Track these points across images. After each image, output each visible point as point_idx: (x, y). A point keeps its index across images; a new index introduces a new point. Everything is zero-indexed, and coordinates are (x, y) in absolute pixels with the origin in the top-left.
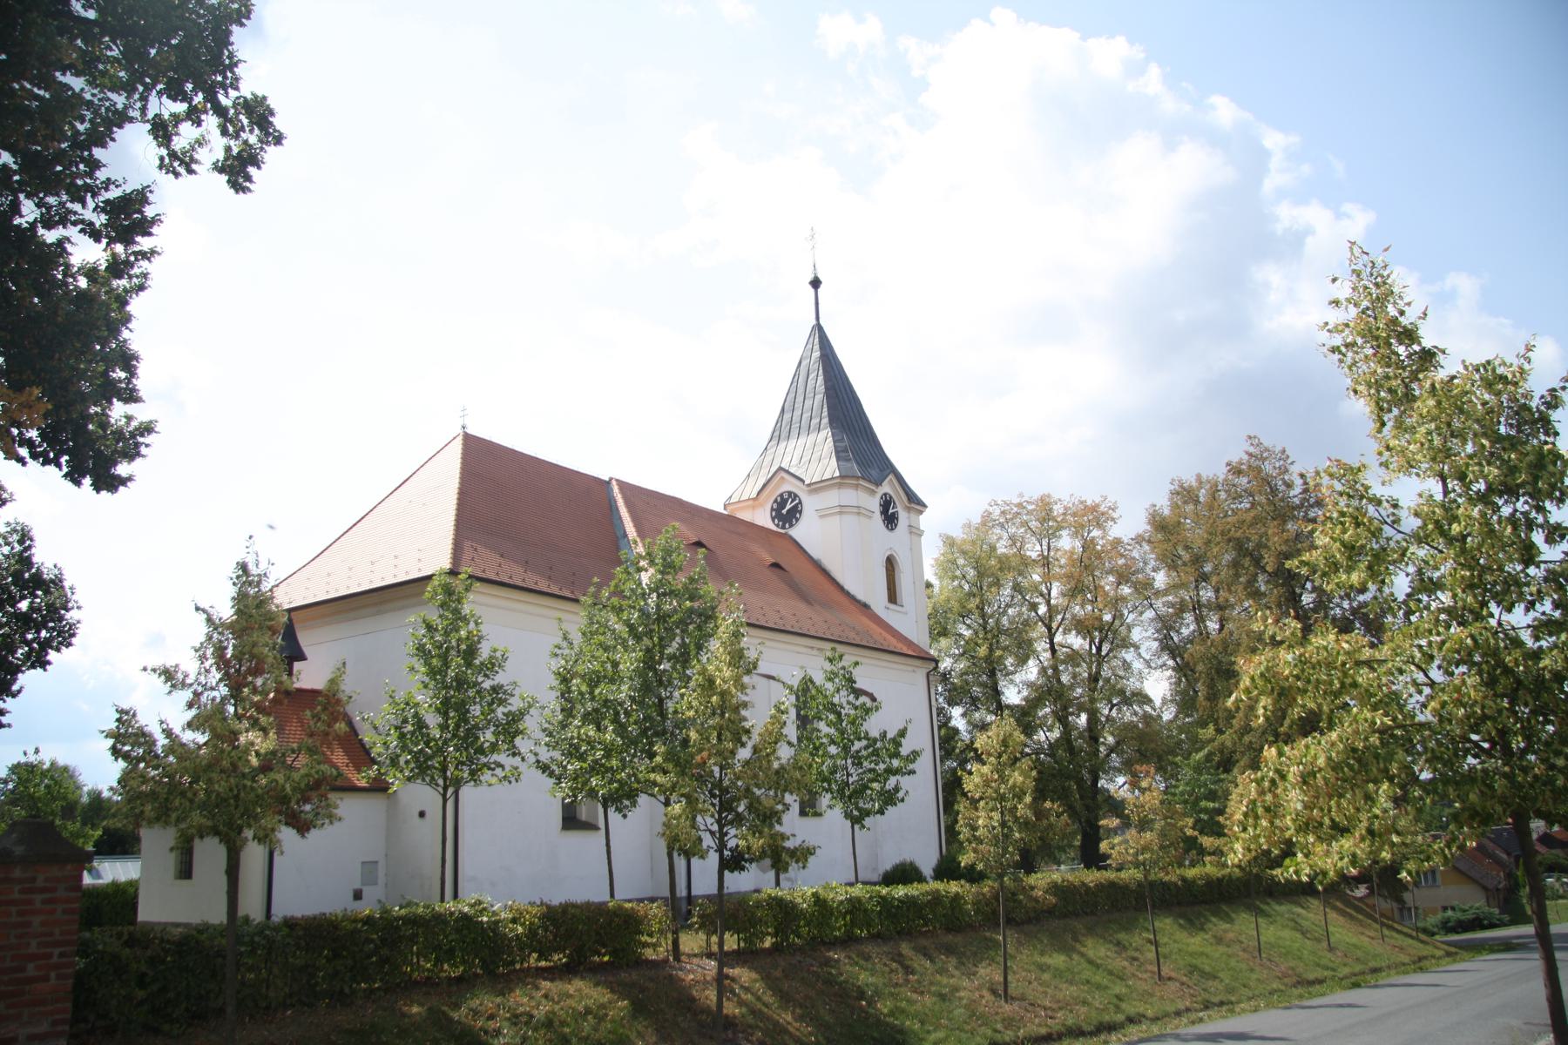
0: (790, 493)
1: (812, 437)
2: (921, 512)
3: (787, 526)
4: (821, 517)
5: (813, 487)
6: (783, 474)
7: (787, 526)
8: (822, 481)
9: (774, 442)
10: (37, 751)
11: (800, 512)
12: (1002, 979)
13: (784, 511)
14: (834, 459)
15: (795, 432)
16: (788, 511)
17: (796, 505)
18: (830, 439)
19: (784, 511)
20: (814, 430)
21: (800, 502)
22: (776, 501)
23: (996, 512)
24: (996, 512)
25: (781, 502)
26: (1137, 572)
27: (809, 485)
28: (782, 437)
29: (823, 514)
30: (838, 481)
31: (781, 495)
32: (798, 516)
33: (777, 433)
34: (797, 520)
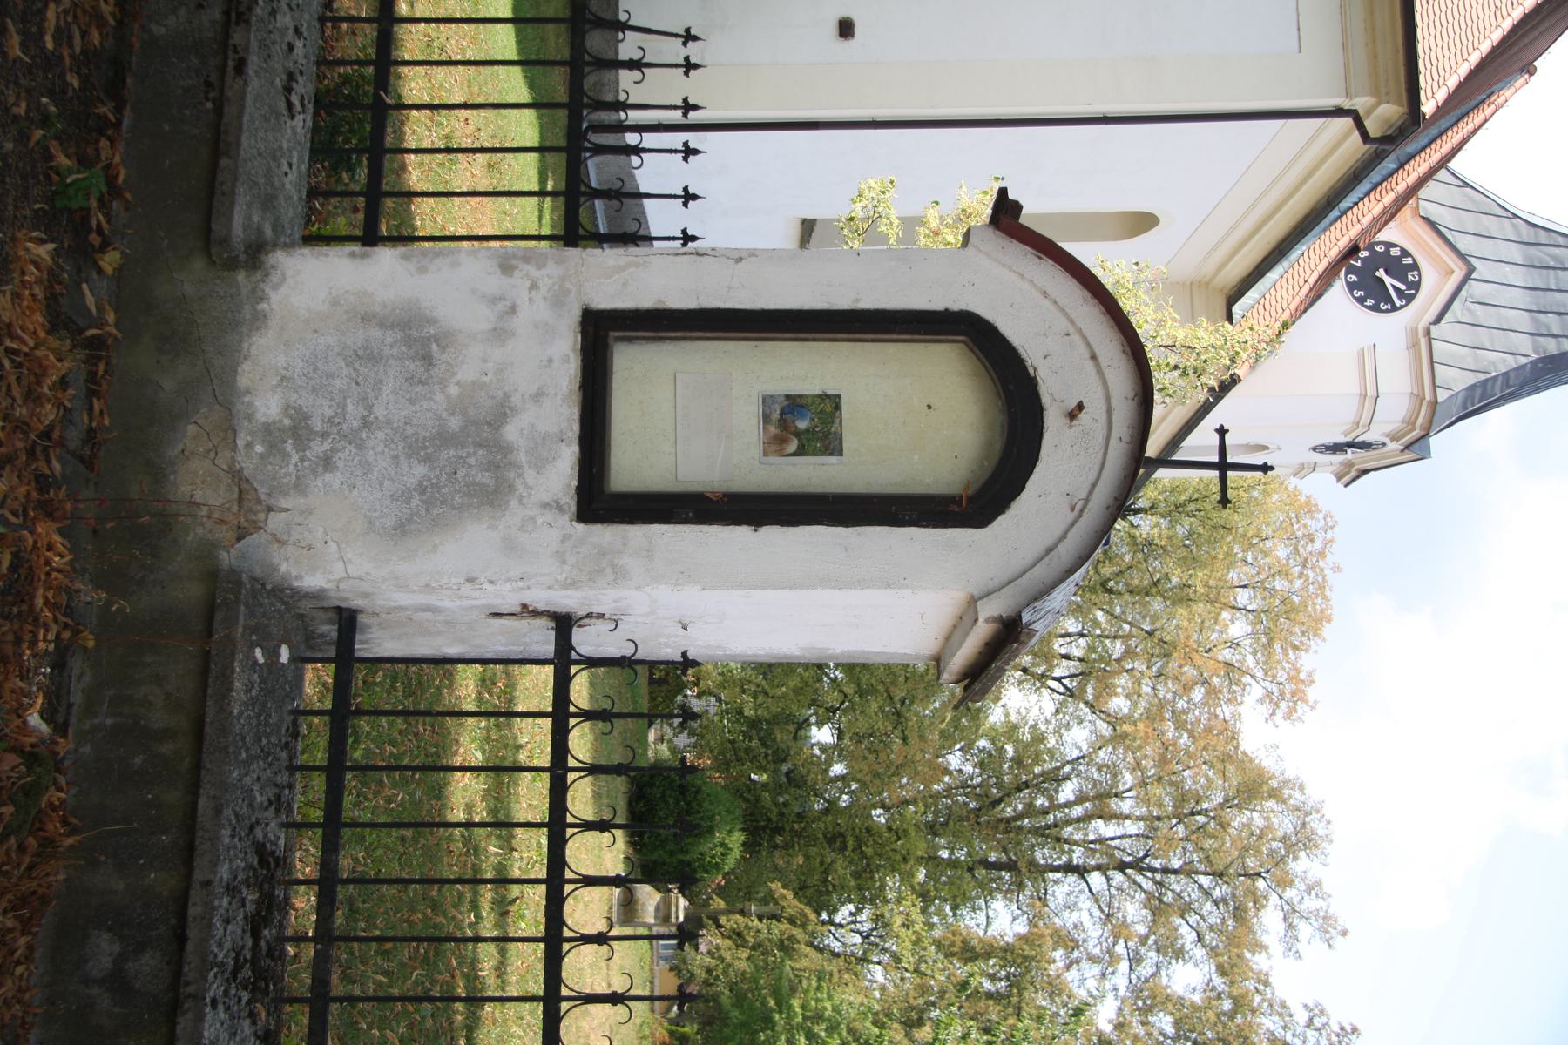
0: (1416, 286)
1: (1523, 321)
2: (1339, 478)
3: (1353, 278)
4: (1362, 353)
5: (1423, 342)
6: (1459, 274)
7: (1353, 278)
8: (1432, 362)
9: (1527, 234)
10: (985, 193)
11: (1375, 308)
12: (418, 15)
13: (1381, 273)
14: (1472, 379)
15: (1536, 279)
16: (1381, 281)
17: (1389, 300)
18: (1512, 362)
19: (1381, 273)
20: (1535, 321)
21: (1394, 308)
22: (1405, 253)
23: (1314, 525)
24: (1314, 525)
25: (1401, 265)
26: (1256, 1033)
27: (1428, 332)
28: (1533, 250)
29: (1367, 359)
30: (1428, 396)
31: (1415, 266)
32: (1369, 302)
33: (1543, 237)
34: (1361, 300)
